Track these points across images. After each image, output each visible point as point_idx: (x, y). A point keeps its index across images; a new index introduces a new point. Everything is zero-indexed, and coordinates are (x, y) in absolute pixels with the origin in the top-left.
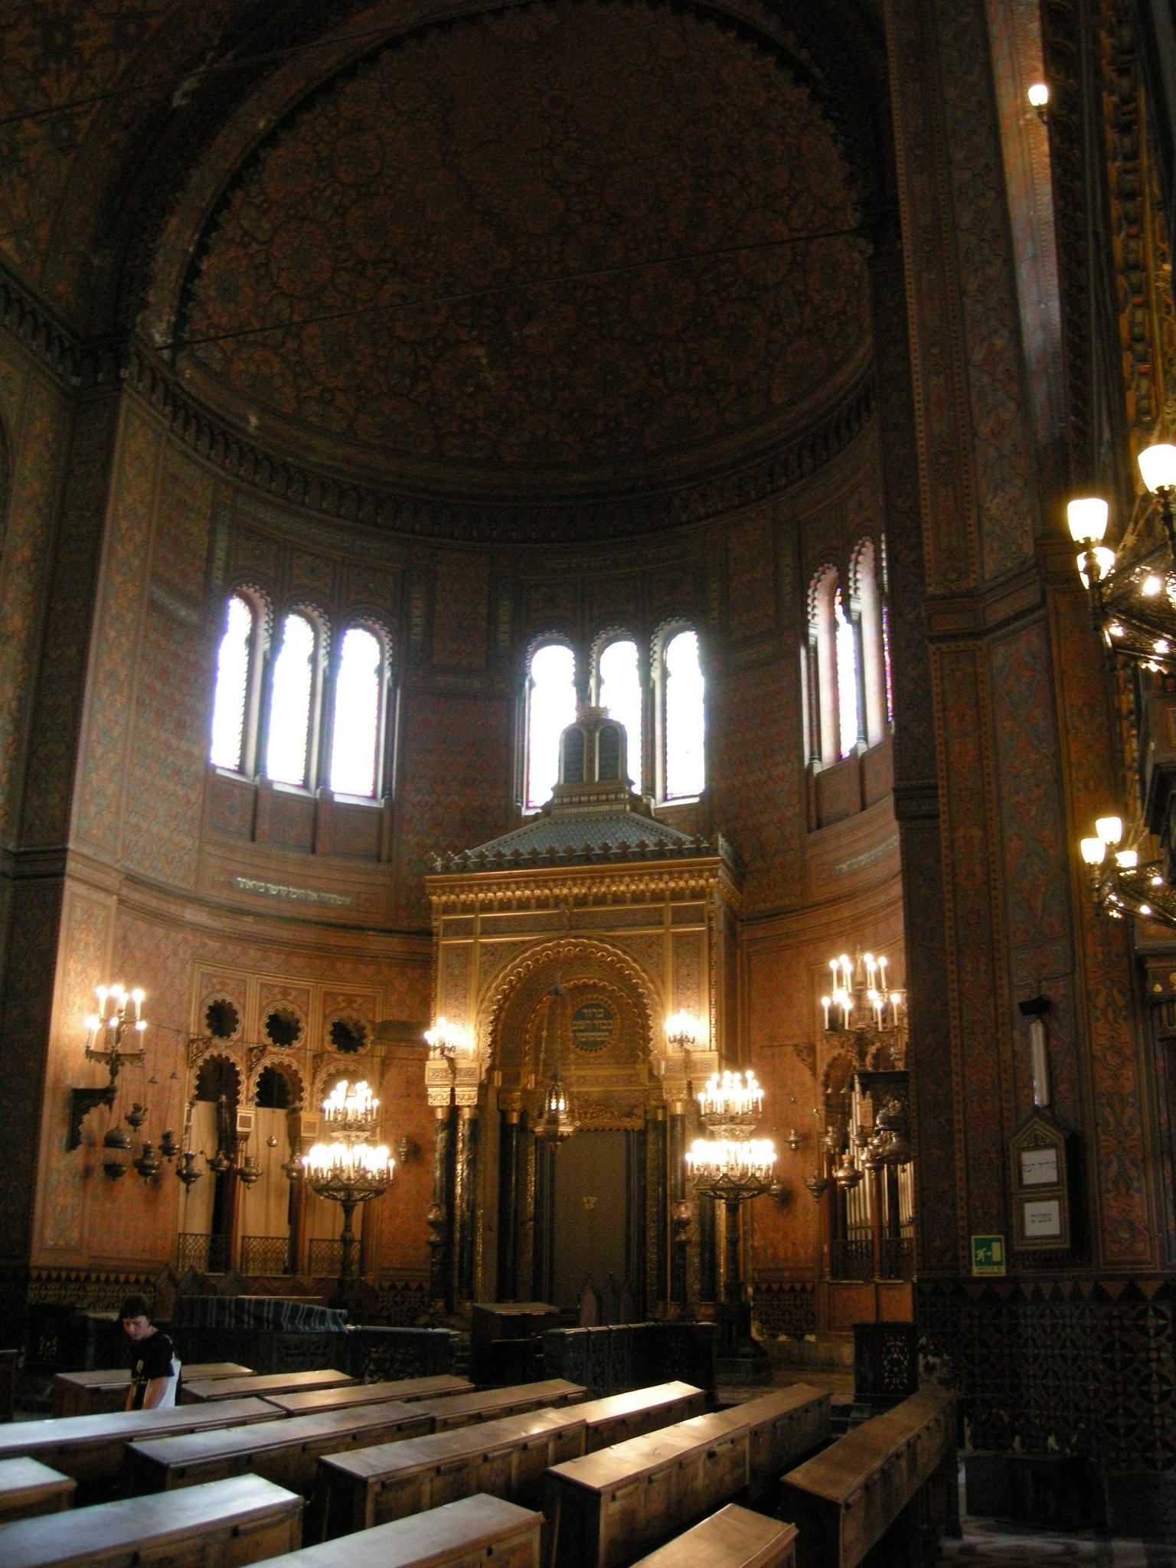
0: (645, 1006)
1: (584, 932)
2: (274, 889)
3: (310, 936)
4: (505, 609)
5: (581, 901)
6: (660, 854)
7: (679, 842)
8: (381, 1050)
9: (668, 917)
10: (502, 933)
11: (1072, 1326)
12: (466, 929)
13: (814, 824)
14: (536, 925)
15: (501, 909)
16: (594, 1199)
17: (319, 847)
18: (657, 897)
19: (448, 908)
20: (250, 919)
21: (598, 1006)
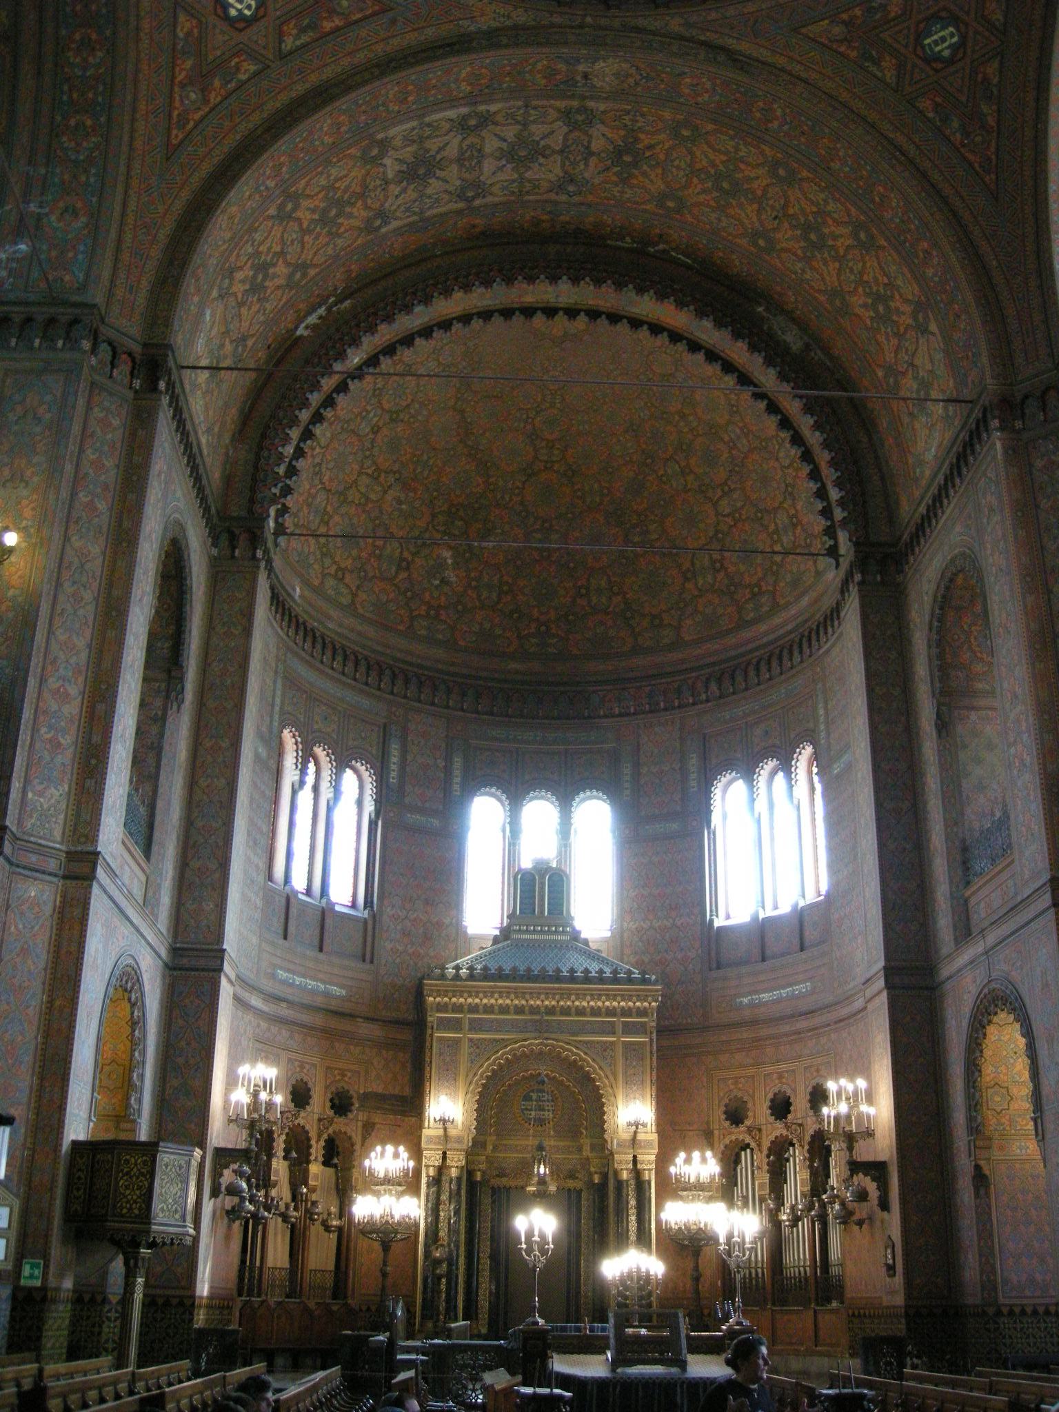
0: (601, 1096)
1: (553, 1036)
2: (298, 980)
3: (319, 1020)
4: (458, 762)
5: (551, 1011)
6: (616, 980)
7: (629, 972)
8: (362, 1116)
9: (619, 1029)
11: (1041, 1338)
12: (456, 1025)
13: (714, 966)
14: (514, 1026)
15: (485, 1012)
17: (325, 948)
18: (611, 1012)
19: (441, 1008)
20: (284, 1005)
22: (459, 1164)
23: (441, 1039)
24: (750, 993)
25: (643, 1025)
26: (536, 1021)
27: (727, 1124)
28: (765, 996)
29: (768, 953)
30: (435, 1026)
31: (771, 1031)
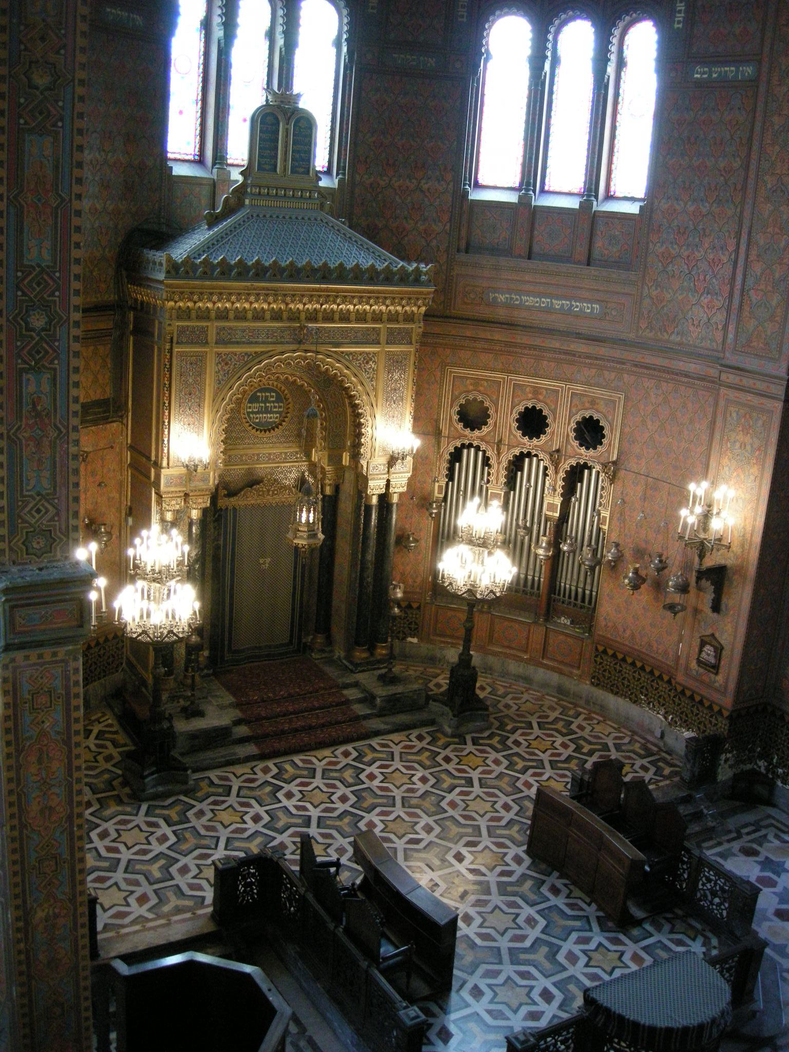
5: (313, 317)
9: (383, 338)
10: (238, 343)
13: (463, 245)
16: (268, 560)
19: (184, 314)
21: (270, 390)
22: (204, 506)
23: (181, 354)
24: (510, 291)
25: (409, 333)
26: (295, 329)
27: (460, 426)
28: (530, 301)
29: (536, 248)
30: (175, 340)
31: (537, 341)
